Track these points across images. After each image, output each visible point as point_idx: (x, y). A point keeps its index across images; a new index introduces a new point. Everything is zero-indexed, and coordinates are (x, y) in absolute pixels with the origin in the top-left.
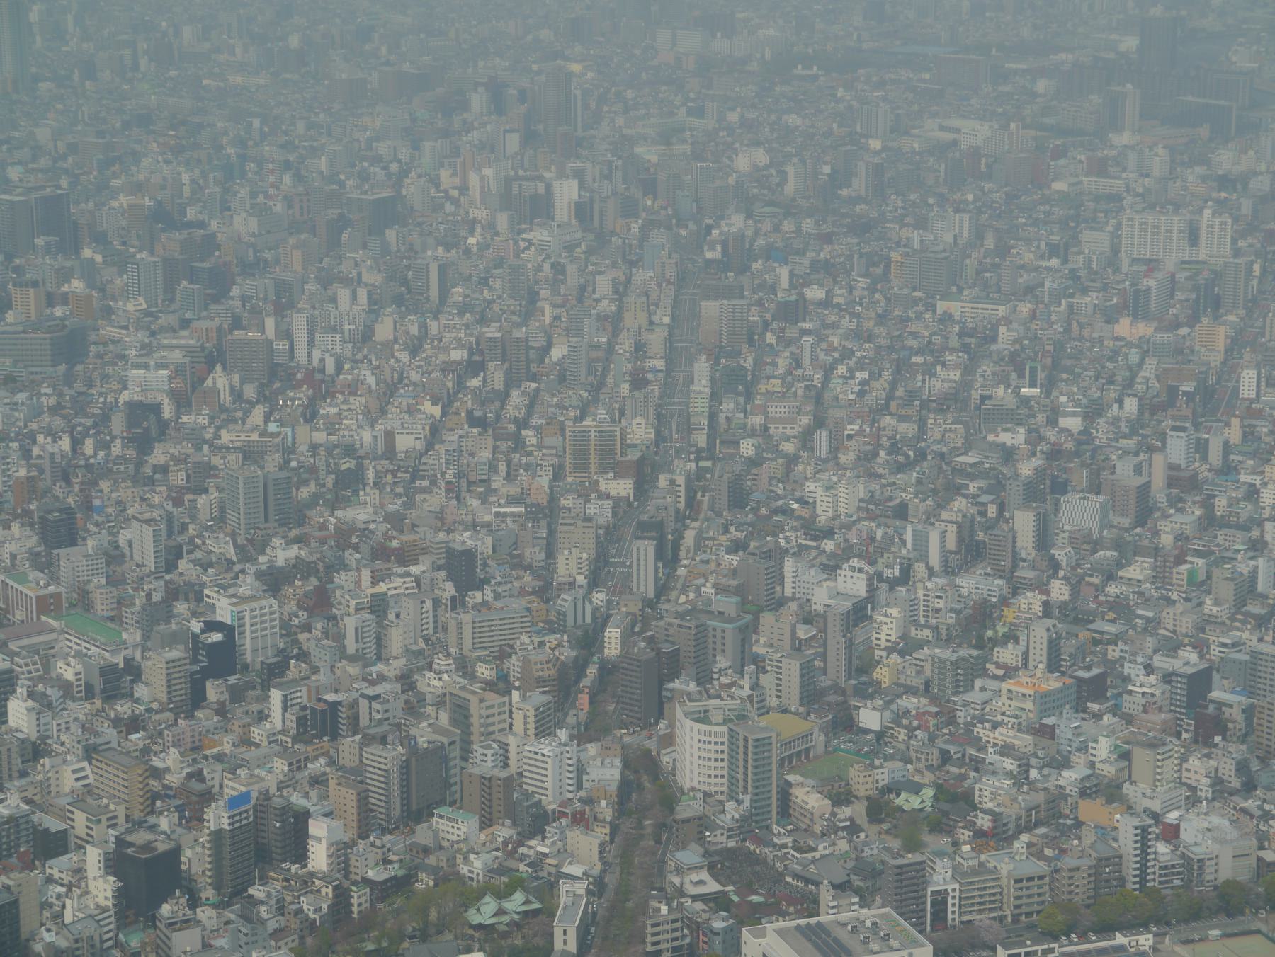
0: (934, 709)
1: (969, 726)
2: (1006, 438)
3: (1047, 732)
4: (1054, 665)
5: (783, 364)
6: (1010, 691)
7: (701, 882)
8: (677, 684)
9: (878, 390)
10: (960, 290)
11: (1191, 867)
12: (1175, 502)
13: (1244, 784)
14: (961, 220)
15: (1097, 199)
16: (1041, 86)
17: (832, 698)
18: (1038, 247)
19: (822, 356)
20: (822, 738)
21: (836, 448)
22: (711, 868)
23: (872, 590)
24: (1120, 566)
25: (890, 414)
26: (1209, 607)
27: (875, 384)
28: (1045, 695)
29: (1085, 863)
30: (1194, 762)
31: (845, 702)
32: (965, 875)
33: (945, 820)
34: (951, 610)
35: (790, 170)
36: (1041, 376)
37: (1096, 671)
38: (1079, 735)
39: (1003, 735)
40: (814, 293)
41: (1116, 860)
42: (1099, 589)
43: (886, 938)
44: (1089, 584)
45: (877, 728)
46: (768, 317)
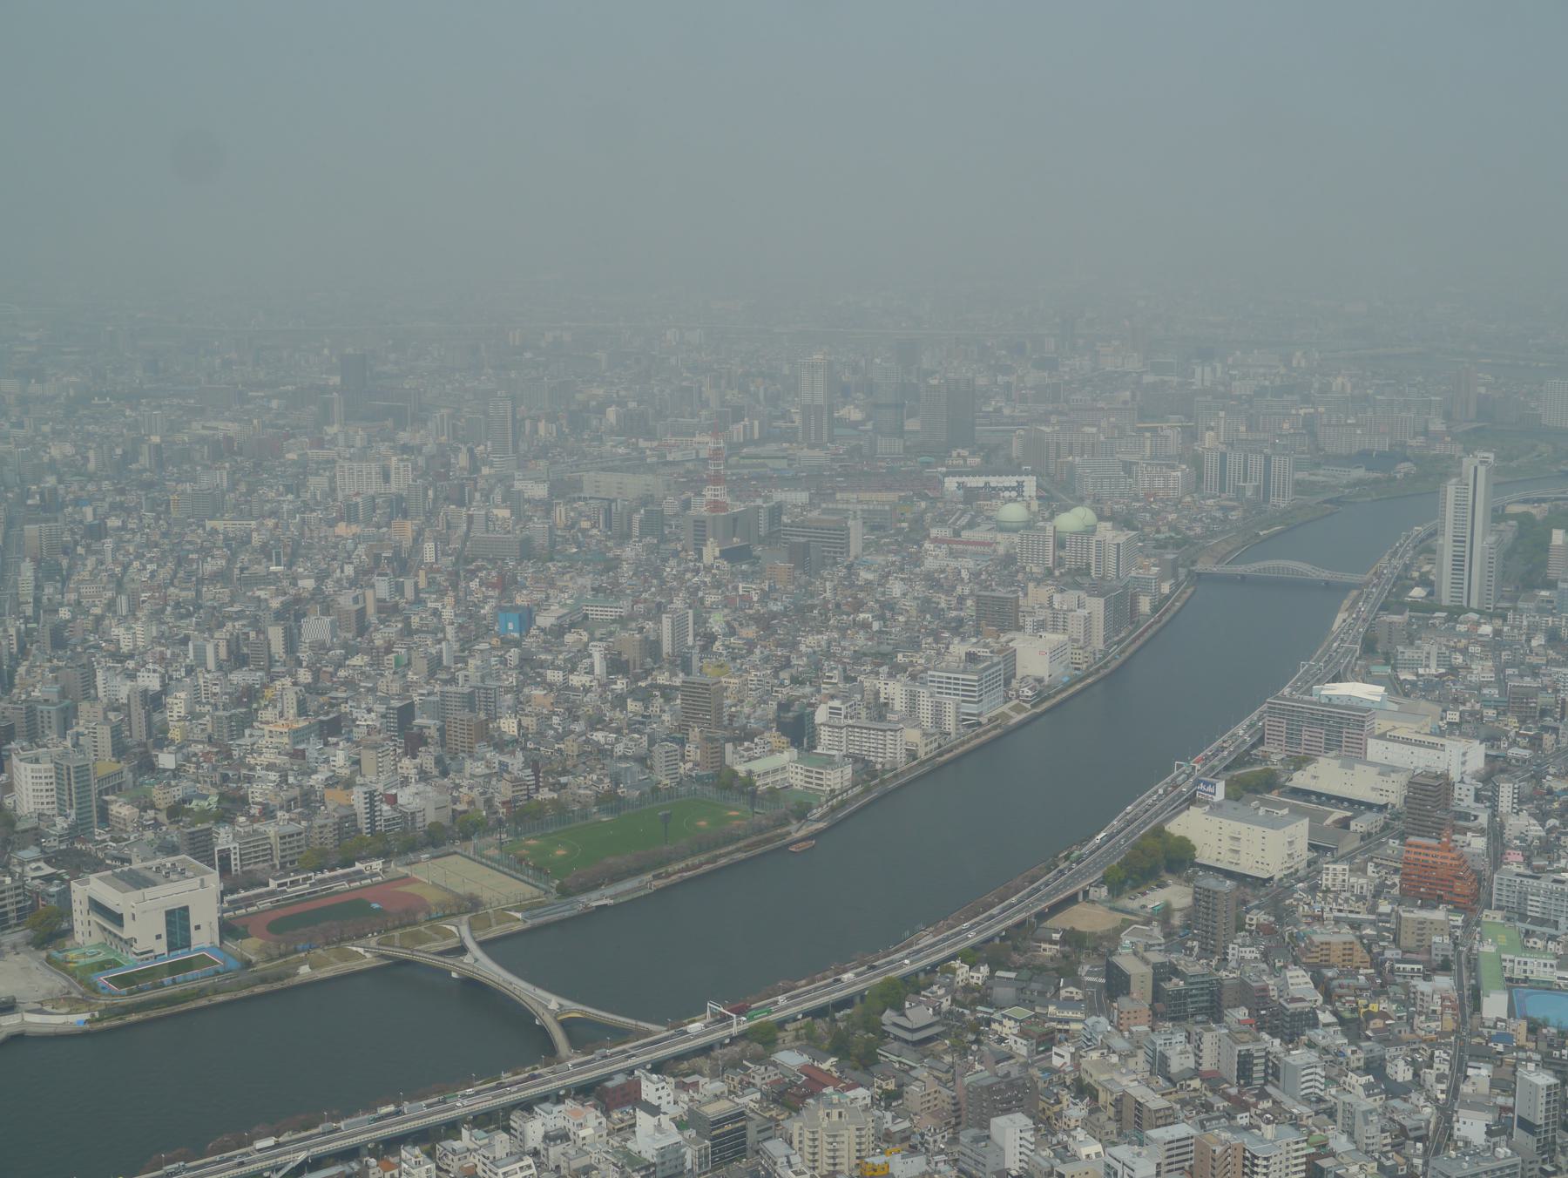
0: (215, 750)
1: (242, 759)
2: (262, 594)
3: (298, 755)
4: (302, 711)
5: (91, 562)
6: (271, 732)
7: (38, 869)
8: (13, 745)
9: (163, 574)
10: (222, 515)
11: (408, 818)
12: (382, 622)
13: (441, 772)
14: (221, 474)
15: (318, 463)
16: (274, 404)
17: (137, 750)
18: (278, 490)
19: (121, 558)
20: (130, 775)
21: (134, 606)
22: (48, 862)
23: (164, 685)
24: (346, 658)
25: (174, 586)
26: (411, 676)
27: (162, 571)
28: (297, 731)
29: (330, 821)
30: (406, 762)
31: (147, 752)
32: (242, 838)
33: (227, 815)
34: (226, 694)
35: (91, 454)
36: (284, 559)
37: (332, 716)
38: (323, 754)
39: (269, 757)
40: (113, 522)
41: (352, 817)
42: (333, 675)
43: (183, 872)
44: (325, 672)
45: (173, 767)
46: (78, 537)
